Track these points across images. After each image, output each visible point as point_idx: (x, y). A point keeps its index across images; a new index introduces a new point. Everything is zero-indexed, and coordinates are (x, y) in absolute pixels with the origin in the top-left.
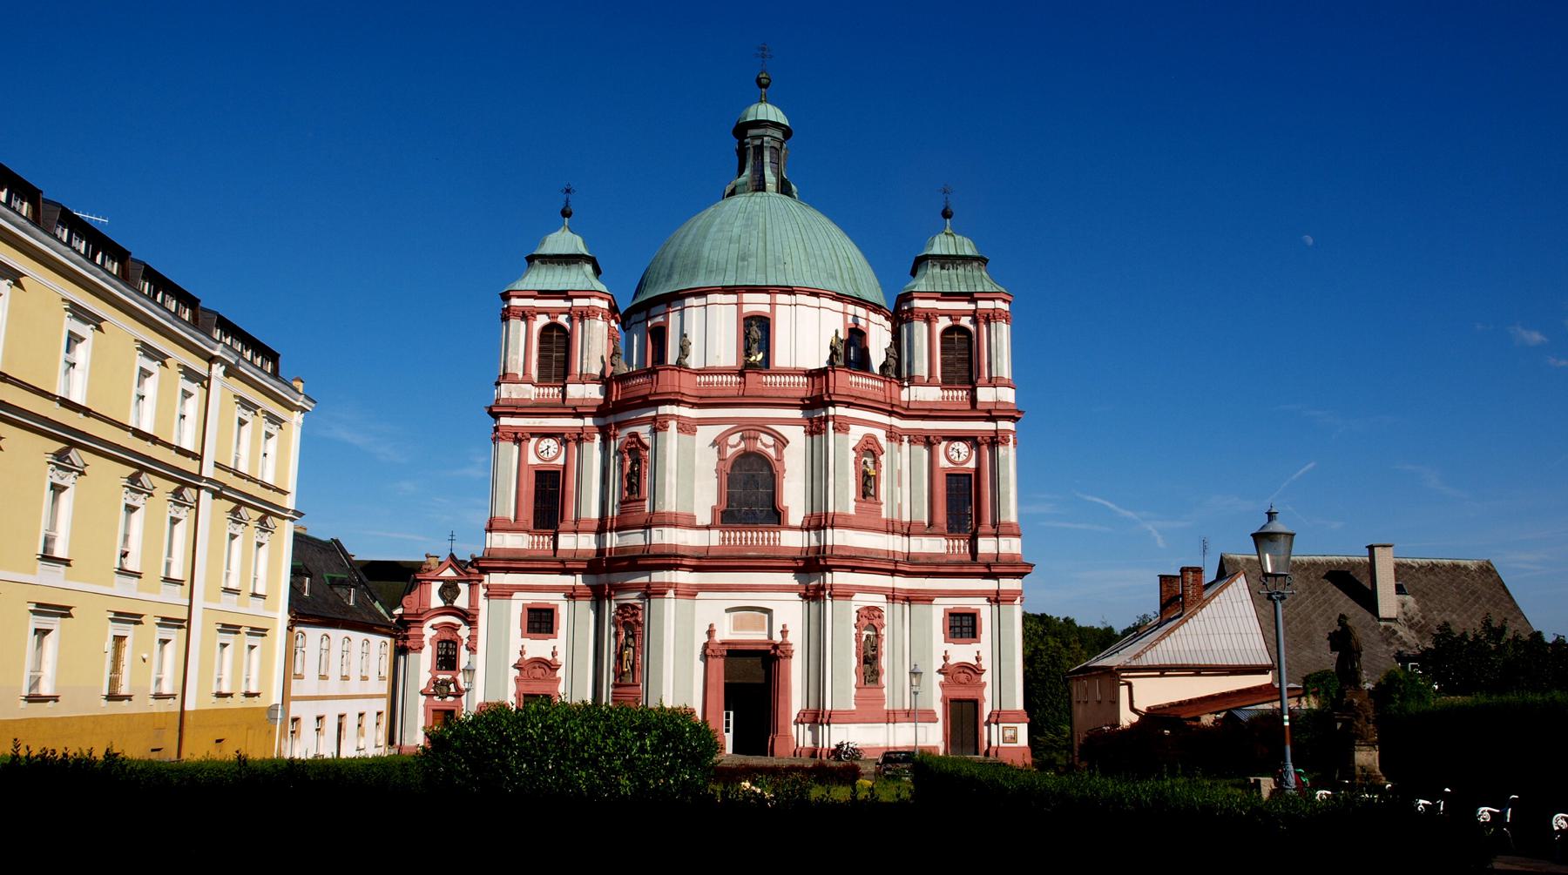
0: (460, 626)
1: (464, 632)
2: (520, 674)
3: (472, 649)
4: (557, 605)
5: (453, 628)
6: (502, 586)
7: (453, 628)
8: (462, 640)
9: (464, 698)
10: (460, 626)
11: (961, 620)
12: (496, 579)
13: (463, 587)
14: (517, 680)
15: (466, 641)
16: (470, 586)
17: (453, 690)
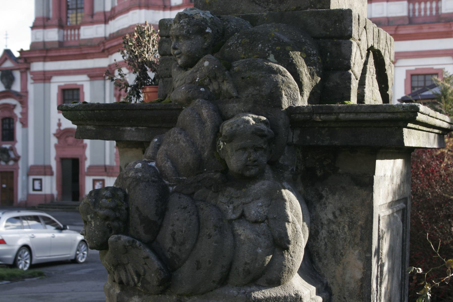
0: (15, 106)
1: (18, 111)
2: (59, 142)
3: (25, 124)
4: (82, 86)
5: (12, 107)
6: (44, 73)
7: (12, 107)
8: (16, 116)
9: (20, 163)
10: (15, 106)
11: (425, 81)
12: (37, 66)
13: (17, 75)
14: (56, 146)
15: (19, 116)
16: (22, 73)
17: (12, 155)
